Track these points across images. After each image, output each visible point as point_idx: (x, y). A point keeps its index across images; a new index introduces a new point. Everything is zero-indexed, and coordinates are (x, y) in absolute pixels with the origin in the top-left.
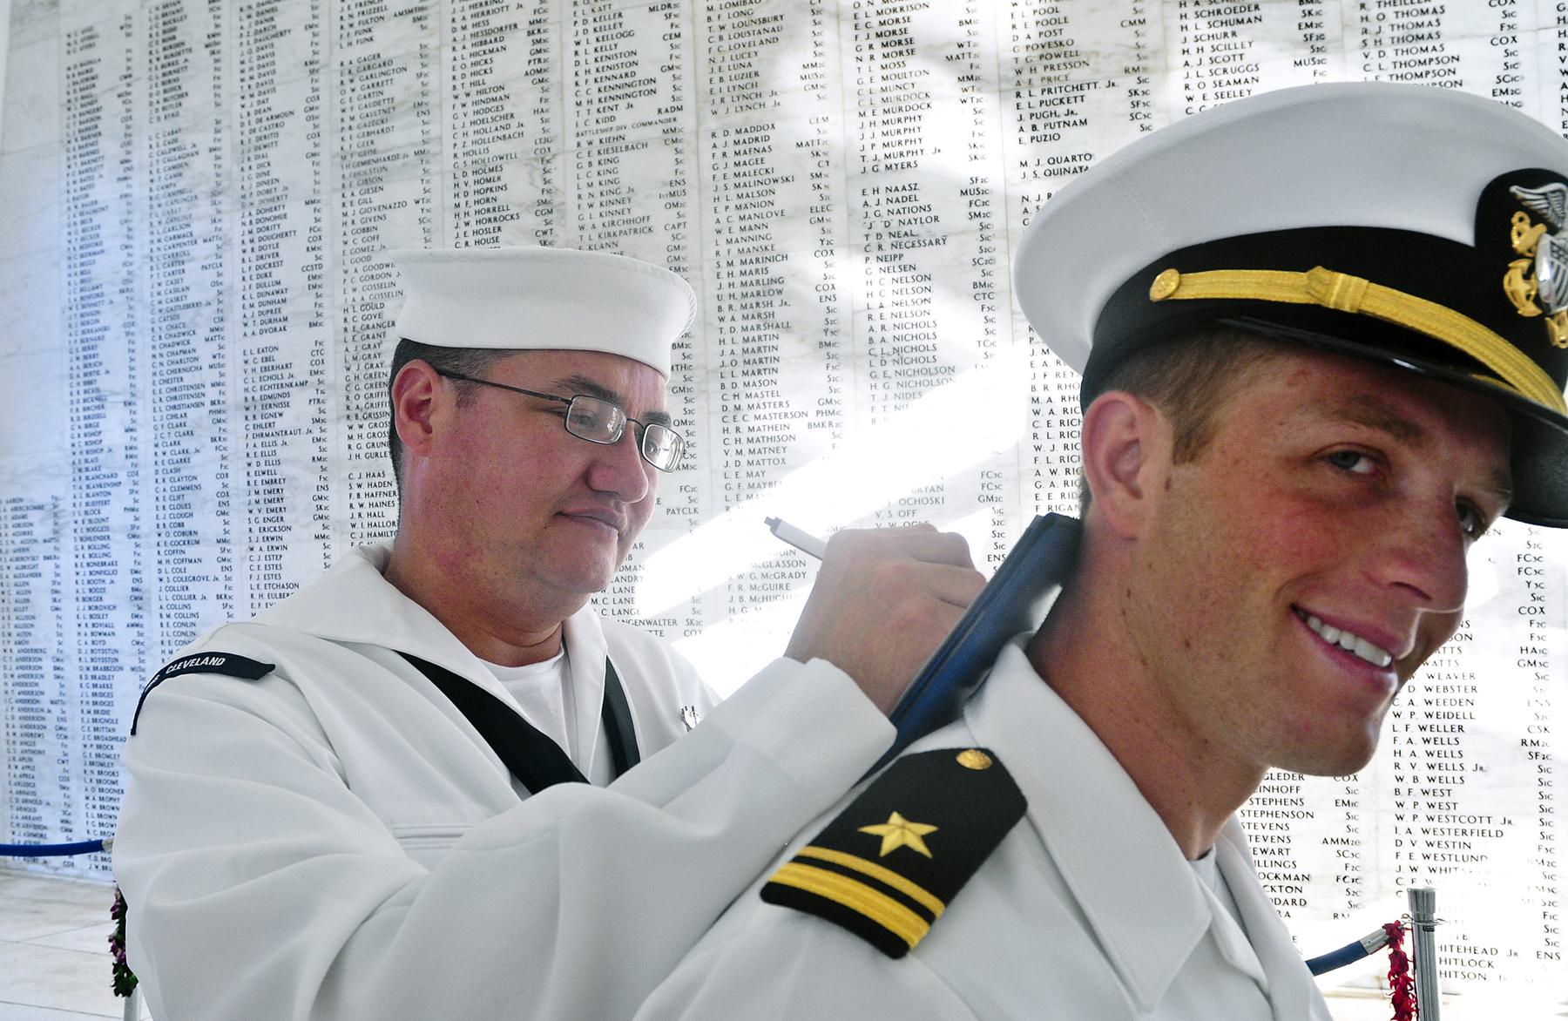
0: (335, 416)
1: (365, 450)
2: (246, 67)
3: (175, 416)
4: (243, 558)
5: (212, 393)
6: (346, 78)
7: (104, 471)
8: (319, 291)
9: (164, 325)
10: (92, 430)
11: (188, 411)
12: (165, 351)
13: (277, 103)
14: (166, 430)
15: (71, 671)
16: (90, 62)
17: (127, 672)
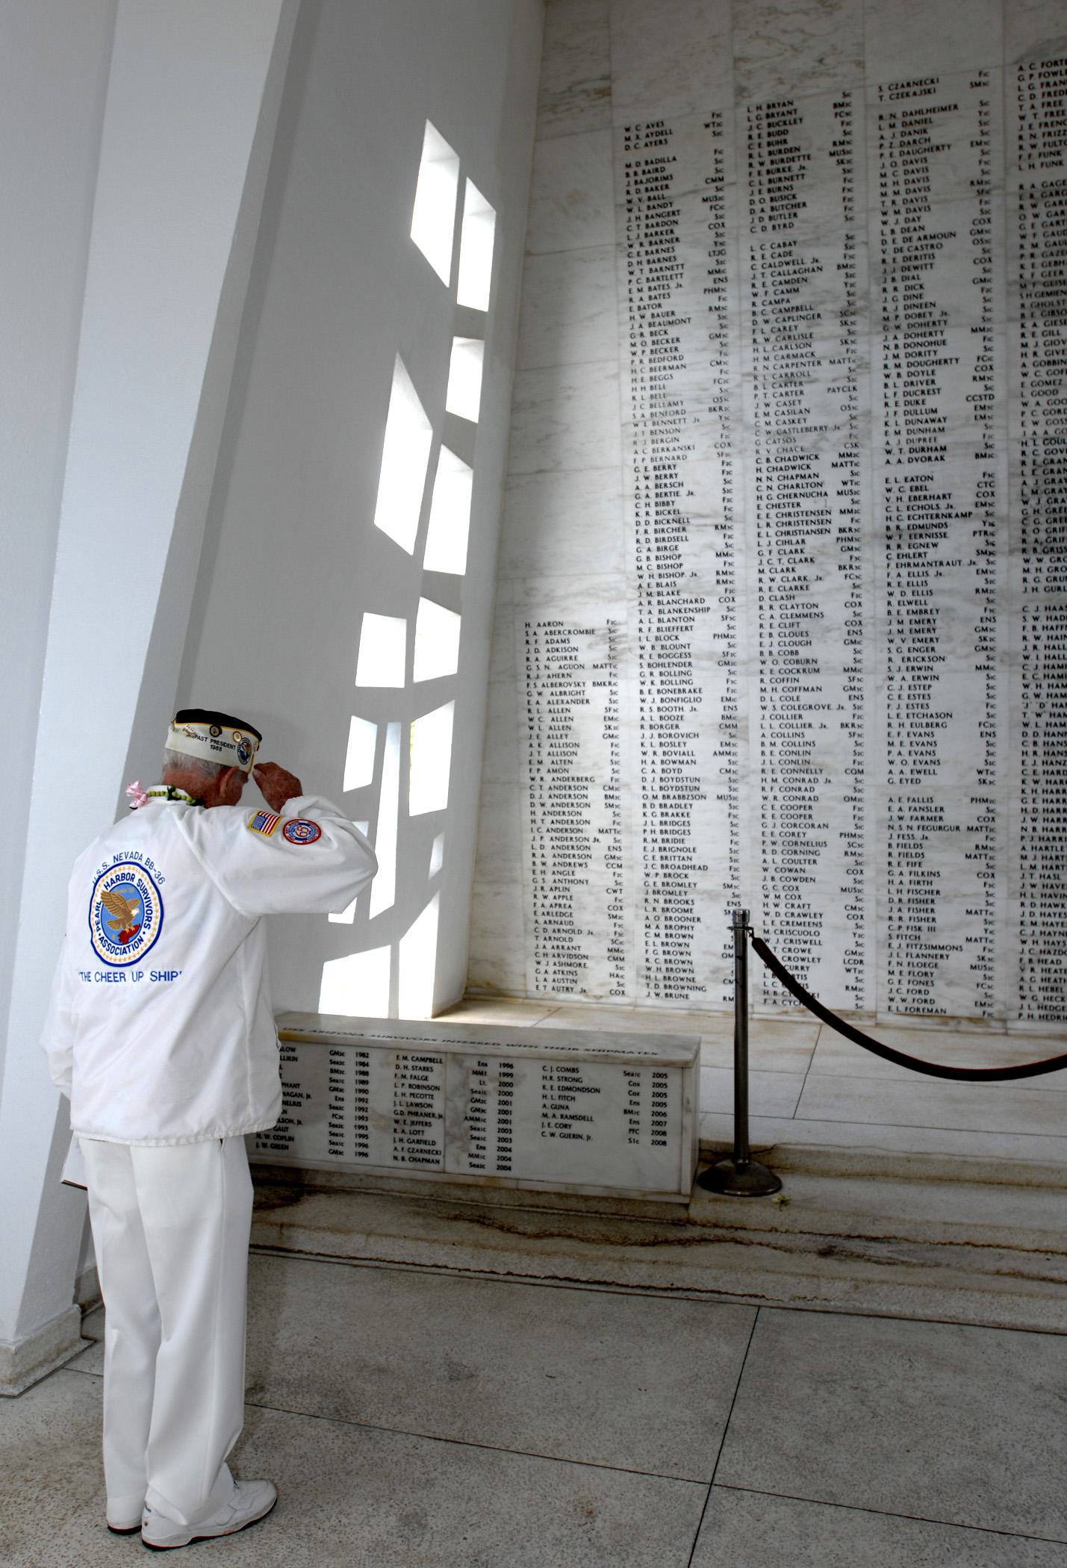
0: (1006, 549)
1: (1044, 583)
2: (889, 180)
3: (790, 542)
4: (878, 688)
5: (845, 521)
6: (1027, 203)
7: (684, 596)
8: (990, 422)
9: (773, 448)
10: (668, 552)
11: (806, 537)
12: (775, 475)
13: (932, 222)
14: (775, 556)
15: (630, 801)
16: (662, 160)
17: (711, 802)
